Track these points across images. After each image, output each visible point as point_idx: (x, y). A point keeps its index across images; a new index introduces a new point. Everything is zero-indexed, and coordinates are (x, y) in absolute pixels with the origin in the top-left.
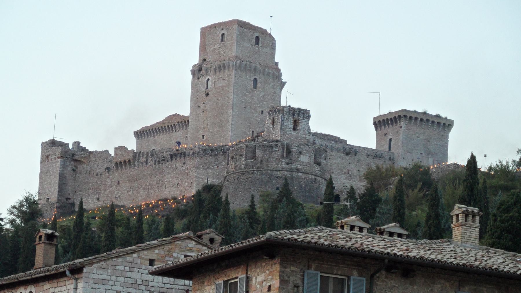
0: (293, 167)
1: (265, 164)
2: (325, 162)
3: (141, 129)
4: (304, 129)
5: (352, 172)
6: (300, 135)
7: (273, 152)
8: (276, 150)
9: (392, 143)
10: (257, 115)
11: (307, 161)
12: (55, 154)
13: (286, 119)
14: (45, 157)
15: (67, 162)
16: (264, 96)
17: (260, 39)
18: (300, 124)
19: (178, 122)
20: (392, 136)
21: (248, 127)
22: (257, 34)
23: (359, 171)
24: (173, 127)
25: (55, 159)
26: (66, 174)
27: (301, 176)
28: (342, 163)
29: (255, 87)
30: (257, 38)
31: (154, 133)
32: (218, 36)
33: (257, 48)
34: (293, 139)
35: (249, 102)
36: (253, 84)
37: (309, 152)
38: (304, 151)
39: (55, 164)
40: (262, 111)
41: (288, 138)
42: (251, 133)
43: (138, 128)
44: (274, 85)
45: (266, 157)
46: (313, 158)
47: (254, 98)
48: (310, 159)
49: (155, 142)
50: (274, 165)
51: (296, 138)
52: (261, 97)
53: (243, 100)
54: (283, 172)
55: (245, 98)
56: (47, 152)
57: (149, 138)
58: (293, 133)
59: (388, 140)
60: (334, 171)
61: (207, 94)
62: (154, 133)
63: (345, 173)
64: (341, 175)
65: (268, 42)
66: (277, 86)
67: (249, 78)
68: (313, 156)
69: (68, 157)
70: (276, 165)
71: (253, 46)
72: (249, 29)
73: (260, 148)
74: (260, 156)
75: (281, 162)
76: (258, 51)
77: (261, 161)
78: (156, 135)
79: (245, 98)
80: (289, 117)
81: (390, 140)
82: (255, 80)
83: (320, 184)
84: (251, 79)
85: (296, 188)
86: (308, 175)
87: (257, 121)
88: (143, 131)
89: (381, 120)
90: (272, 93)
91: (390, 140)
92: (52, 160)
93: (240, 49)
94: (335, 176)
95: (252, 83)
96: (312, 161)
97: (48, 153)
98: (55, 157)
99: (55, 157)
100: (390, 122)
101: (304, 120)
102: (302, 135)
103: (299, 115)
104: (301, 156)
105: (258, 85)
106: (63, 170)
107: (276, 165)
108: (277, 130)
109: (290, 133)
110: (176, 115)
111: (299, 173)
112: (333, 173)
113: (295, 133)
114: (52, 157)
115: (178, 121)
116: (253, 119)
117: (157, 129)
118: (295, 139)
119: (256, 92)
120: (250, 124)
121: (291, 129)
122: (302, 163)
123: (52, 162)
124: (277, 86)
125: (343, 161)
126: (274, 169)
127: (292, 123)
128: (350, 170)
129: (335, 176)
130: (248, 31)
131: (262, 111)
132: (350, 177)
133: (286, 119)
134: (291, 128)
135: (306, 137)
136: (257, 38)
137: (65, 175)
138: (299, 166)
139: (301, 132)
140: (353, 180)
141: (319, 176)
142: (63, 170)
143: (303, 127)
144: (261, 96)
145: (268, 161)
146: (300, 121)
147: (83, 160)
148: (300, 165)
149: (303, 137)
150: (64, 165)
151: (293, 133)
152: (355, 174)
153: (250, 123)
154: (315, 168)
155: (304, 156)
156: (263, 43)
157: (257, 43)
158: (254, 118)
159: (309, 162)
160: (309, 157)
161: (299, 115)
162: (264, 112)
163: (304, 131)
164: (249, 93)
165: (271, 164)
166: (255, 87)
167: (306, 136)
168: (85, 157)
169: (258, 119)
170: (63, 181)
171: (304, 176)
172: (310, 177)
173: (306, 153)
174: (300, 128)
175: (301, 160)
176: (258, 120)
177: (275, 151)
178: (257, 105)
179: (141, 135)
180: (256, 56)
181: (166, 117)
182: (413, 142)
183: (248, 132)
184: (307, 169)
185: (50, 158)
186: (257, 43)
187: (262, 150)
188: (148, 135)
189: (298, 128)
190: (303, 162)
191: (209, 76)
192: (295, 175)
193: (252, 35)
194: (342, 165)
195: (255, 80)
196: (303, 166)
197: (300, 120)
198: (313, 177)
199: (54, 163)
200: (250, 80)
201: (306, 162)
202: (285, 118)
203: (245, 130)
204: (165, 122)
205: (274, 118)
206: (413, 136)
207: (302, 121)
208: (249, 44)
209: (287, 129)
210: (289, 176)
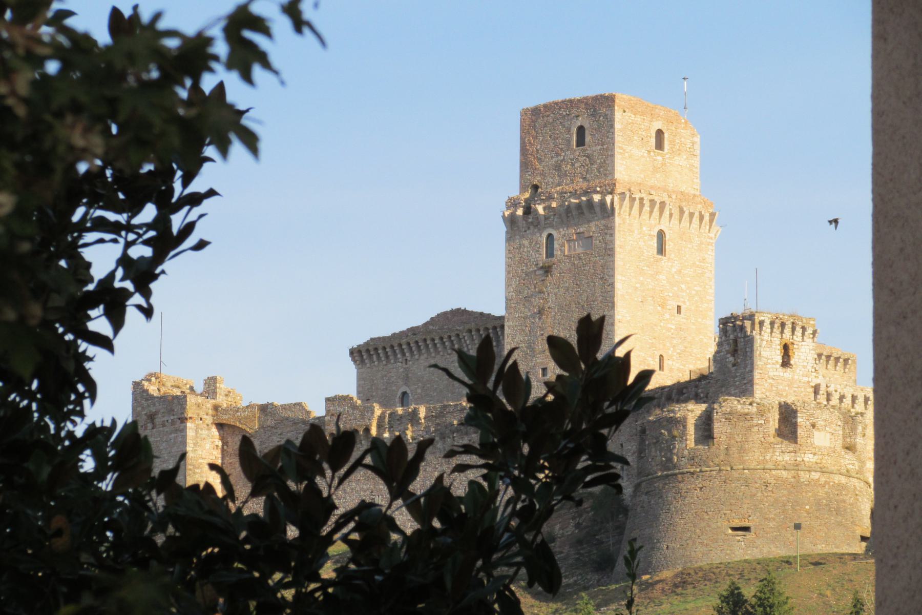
0: (798, 459)
1: (736, 455)
2: (863, 442)
3: (367, 344)
4: (805, 364)
6: (796, 377)
7: (752, 426)
8: (760, 422)
10: (667, 316)
11: (828, 445)
12: (174, 410)
13: (764, 343)
14: (145, 417)
15: (202, 429)
16: (680, 272)
17: (666, 135)
18: (796, 353)
19: (470, 331)
21: (650, 348)
22: (658, 125)
24: (455, 342)
25: (173, 422)
26: (203, 458)
27: (818, 480)
29: (661, 250)
30: (660, 133)
31: (404, 354)
32: (569, 130)
33: (659, 158)
34: (781, 387)
35: (650, 287)
36: (656, 245)
38: (820, 423)
39: (173, 435)
40: (679, 307)
41: (772, 385)
42: (657, 360)
43: (360, 340)
44: (702, 243)
45: (739, 440)
46: (841, 437)
47: (661, 277)
48: (833, 440)
49: (407, 375)
51: (788, 385)
52: (675, 272)
53: (638, 285)
54: (779, 471)
55: (641, 279)
56: (149, 406)
57: (390, 366)
58: (782, 374)
61: (547, 270)
62: (404, 354)
65: (683, 140)
66: (709, 244)
67: (646, 232)
68: (841, 432)
69: (205, 417)
70: (761, 458)
71: (652, 154)
72: (643, 114)
73: (724, 420)
74: (723, 438)
75: (771, 450)
76: (663, 164)
77: (727, 449)
78: (409, 359)
79: (641, 279)
82: (661, 235)
83: (857, 495)
84: (652, 233)
85: (807, 507)
87: (669, 330)
88: (376, 349)
90: (697, 263)
92: (164, 425)
93: (625, 163)
95: (654, 243)
96: (839, 443)
97: (153, 410)
98: (172, 417)
99: (172, 417)
101: (803, 343)
102: (801, 378)
103: (793, 330)
104: (816, 433)
105: (669, 246)
106: (195, 450)
107: (761, 458)
108: (745, 368)
109: (775, 373)
110: (459, 314)
113: (787, 374)
114: (165, 419)
115: (467, 327)
116: (659, 328)
117: (412, 345)
118: (787, 388)
119: (664, 261)
120: (654, 341)
121: (778, 366)
123: (166, 429)
124: (709, 244)
126: (758, 467)
127: (778, 352)
130: (638, 119)
131: (679, 307)
133: (764, 343)
134: (777, 362)
135: (809, 382)
136: (660, 133)
137: (201, 461)
139: (798, 371)
142: (195, 450)
143: (802, 357)
144: (674, 270)
145: (742, 450)
146: (795, 346)
147: (238, 424)
149: (804, 383)
150: (197, 437)
151: (782, 374)
153: (655, 338)
154: (845, 458)
155: (823, 433)
156: (672, 142)
157: (659, 145)
158: (662, 324)
161: (793, 330)
162: (683, 310)
163: (805, 367)
164: (648, 266)
165: (750, 454)
166: (661, 250)
167: (810, 380)
168: (246, 418)
169: (669, 326)
170: (197, 476)
171: (823, 480)
173: (825, 426)
174: (797, 360)
176: (672, 328)
177: (757, 425)
178: (666, 294)
179: (370, 356)
180: (658, 175)
181: (434, 315)
183: (650, 359)
184: (829, 462)
185: (159, 420)
186: (659, 145)
188: (387, 357)
189: (792, 362)
190: (820, 448)
191: (552, 226)
192: (804, 476)
193: (648, 130)
195: (661, 235)
196: (821, 457)
197: (795, 343)
198: (843, 480)
199: (171, 433)
200: (650, 235)
201: (825, 447)
202: (762, 340)
203: (643, 355)
204: (431, 327)
205: (735, 341)
207: (800, 344)
208: (643, 151)
209: (769, 366)
210: (792, 480)
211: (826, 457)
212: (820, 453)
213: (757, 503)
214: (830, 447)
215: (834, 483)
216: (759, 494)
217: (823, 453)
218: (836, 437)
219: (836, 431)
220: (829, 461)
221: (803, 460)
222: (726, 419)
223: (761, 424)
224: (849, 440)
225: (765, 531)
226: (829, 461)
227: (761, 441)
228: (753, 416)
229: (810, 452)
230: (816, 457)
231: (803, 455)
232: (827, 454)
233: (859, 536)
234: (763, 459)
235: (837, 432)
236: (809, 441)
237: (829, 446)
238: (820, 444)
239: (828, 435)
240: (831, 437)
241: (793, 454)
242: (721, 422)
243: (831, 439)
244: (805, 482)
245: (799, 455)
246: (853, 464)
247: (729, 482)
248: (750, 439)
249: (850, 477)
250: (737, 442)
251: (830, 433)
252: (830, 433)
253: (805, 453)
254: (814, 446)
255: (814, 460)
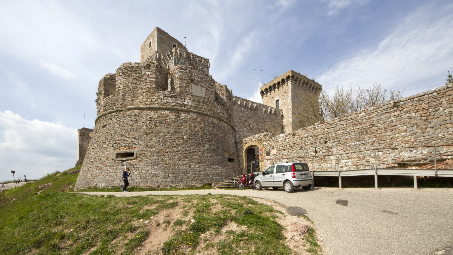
2: (230, 103)
5: (252, 125)
9: (280, 103)
11: (203, 95)
20: (279, 97)
23: (258, 124)
28: (243, 117)
37: (205, 81)
45: (131, 88)
48: (207, 93)
50: (144, 100)
59: (275, 102)
60: (237, 124)
63: (246, 127)
64: (243, 128)
73: (121, 74)
75: (156, 95)
80: (184, 61)
81: (277, 101)
86: (206, 117)
89: (268, 87)
91: (277, 101)
94: (238, 129)
100: (276, 86)
107: (148, 100)
111: (191, 114)
112: (236, 126)
122: (195, 98)
125: (244, 115)
128: (251, 124)
129: (238, 129)
132: (251, 129)
138: (190, 101)
140: (254, 132)
141: (223, 121)
145: (134, 94)
148: (193, 100)
152: (255, 127)
154: (217, 108)
155: (199, 88)
159: (207, 97)
160: (207, 89)
165: (140, 98)
172: (210, 121)
175: (194, 93)
182: (298, 99)
187: (123, 76)
190: (197, 97)
194: (244, 119)
196: (197, 103)
198: (216, 121)
201: (202, 97)
206: (298, 95)
211: (203, 104)
212: (198, 100)
213: (142, 134)
214: (205, 97)
215: (209, 122)
216: (144, 127)
217: (200, 101)
218: (210, 92)
219: (209, 88)
220: (205, 107)
221: (183, 104)
222: (123, 73)
223: (148, 74)
224: (221, 100)
225: (145, 156)
226: (205, 107)
227: (148, 88)
228: (142, 69)
229: (190, 98)
230: (194, 103)
231: (183, 100)
232: (203, 101)
233: (227, 158)
234: (150, 101)
235: (210, 89)
236: (188, 90)
237: (204, 97)
238: (197, 95)
239: (204, 89)
240: (206, 91)
241: (175, 99)
242: (120, 76)
243: (206, 92)
244: (184, 119)
245: (180, 99)
246: (223, 114)
247: (123, 119)
248: (140, 86)
249: (220, 120)
250: (130, 89)
251: (205, 88)
252: (205, 88)
253: (185, 99)
254: (192, 94)
255: (193, 105)
